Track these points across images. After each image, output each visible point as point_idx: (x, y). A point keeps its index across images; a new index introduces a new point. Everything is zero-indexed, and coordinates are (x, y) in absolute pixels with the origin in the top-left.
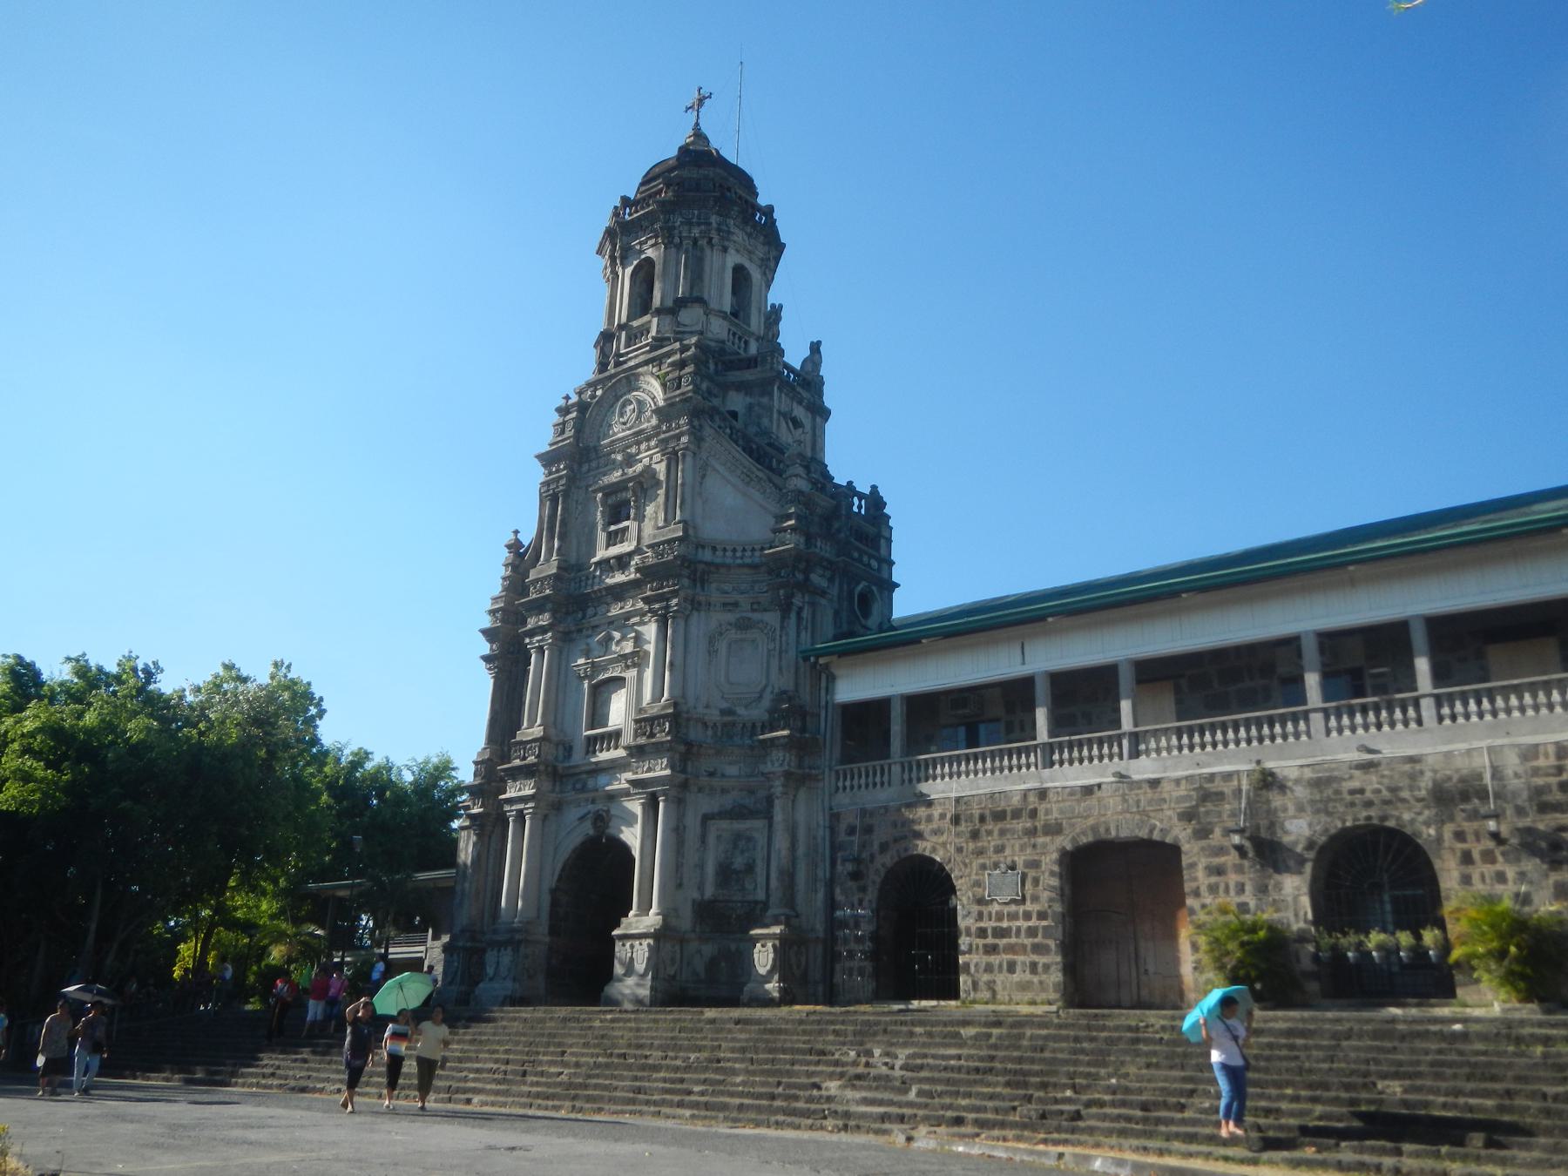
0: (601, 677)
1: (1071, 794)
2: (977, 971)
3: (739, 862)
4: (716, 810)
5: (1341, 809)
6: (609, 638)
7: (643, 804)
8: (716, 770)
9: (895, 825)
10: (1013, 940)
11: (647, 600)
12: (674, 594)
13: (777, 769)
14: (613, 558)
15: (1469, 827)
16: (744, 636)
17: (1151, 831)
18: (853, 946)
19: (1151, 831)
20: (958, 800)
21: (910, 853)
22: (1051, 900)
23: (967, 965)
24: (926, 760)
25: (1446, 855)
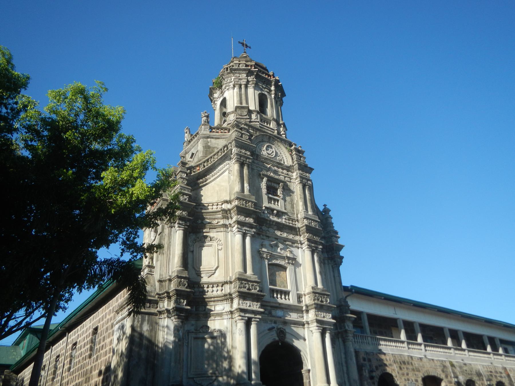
0: (274, 262)
1: (418, 359)
5: (465, 374)
6: (277, 246)
7: (320, 332)
9: (377, 360)
11: (309, 240)
12: (321, 244)
14: (276, 210)
20: (392, 354)
21: (385, 372)
24: (378, 338)
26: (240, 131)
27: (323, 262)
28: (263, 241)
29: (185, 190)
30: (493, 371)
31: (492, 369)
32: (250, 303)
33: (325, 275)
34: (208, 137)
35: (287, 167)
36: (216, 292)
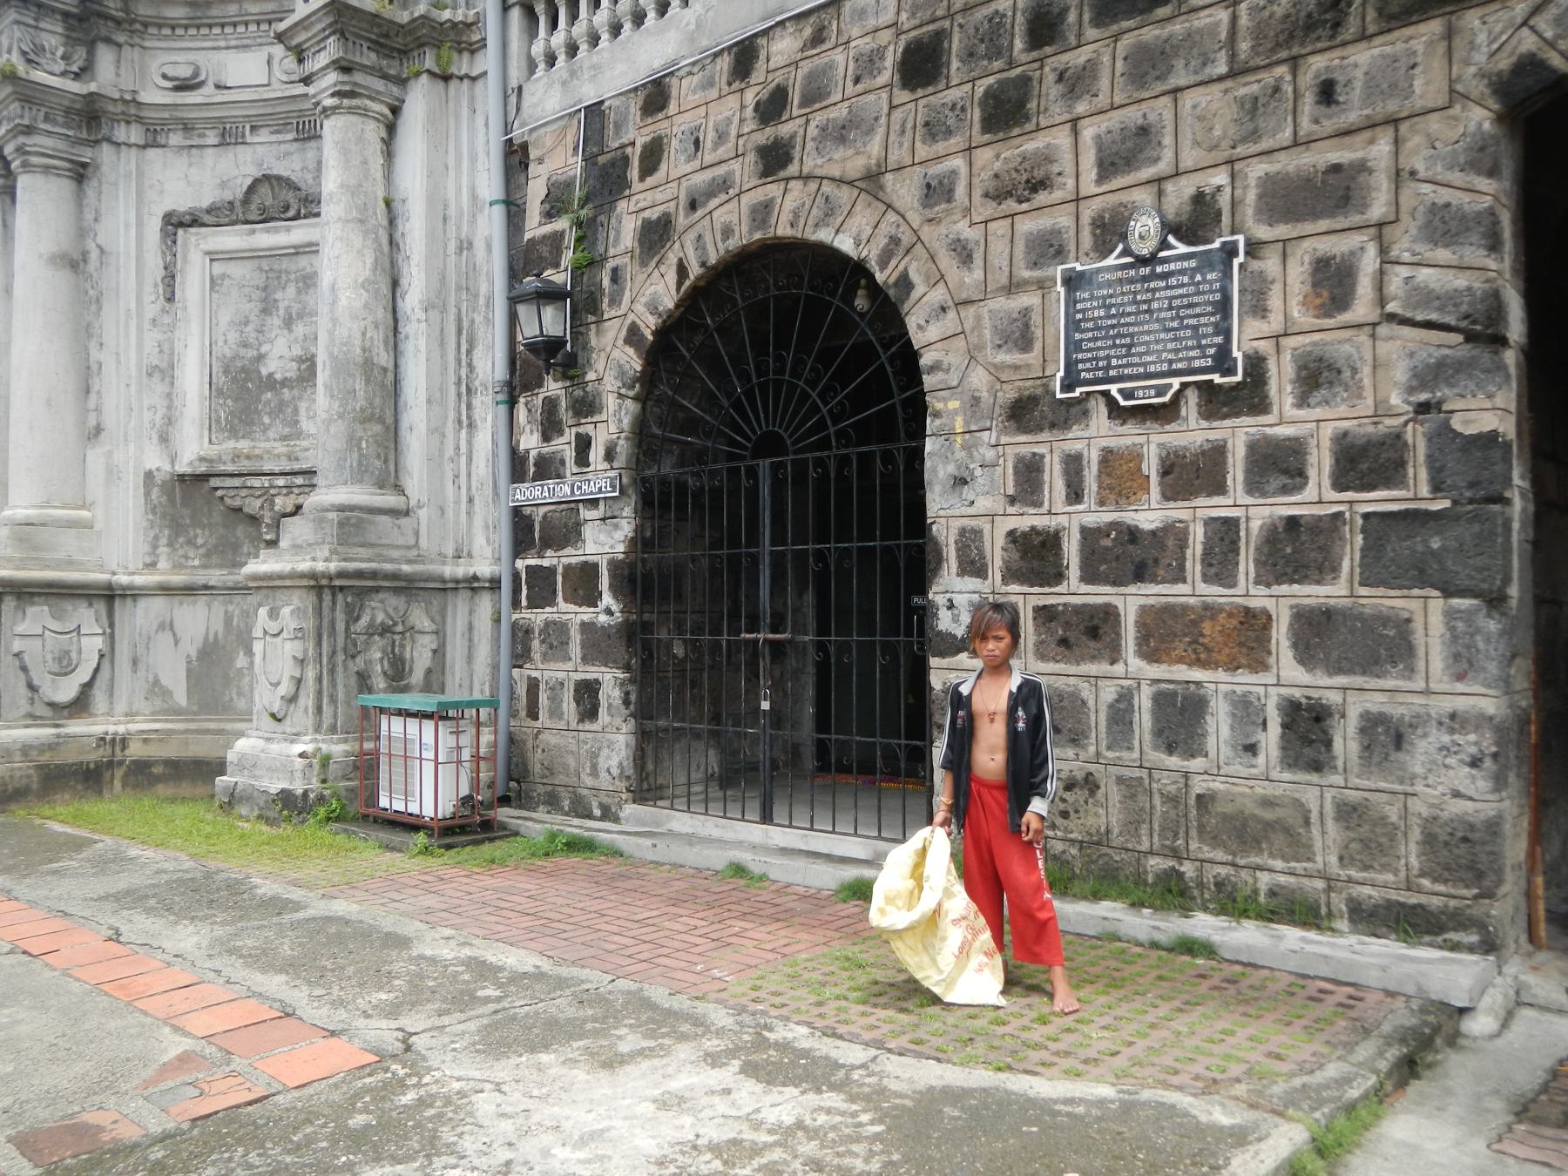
8: (196, 74)
10: (1194, 590)
22: (1431, 375)
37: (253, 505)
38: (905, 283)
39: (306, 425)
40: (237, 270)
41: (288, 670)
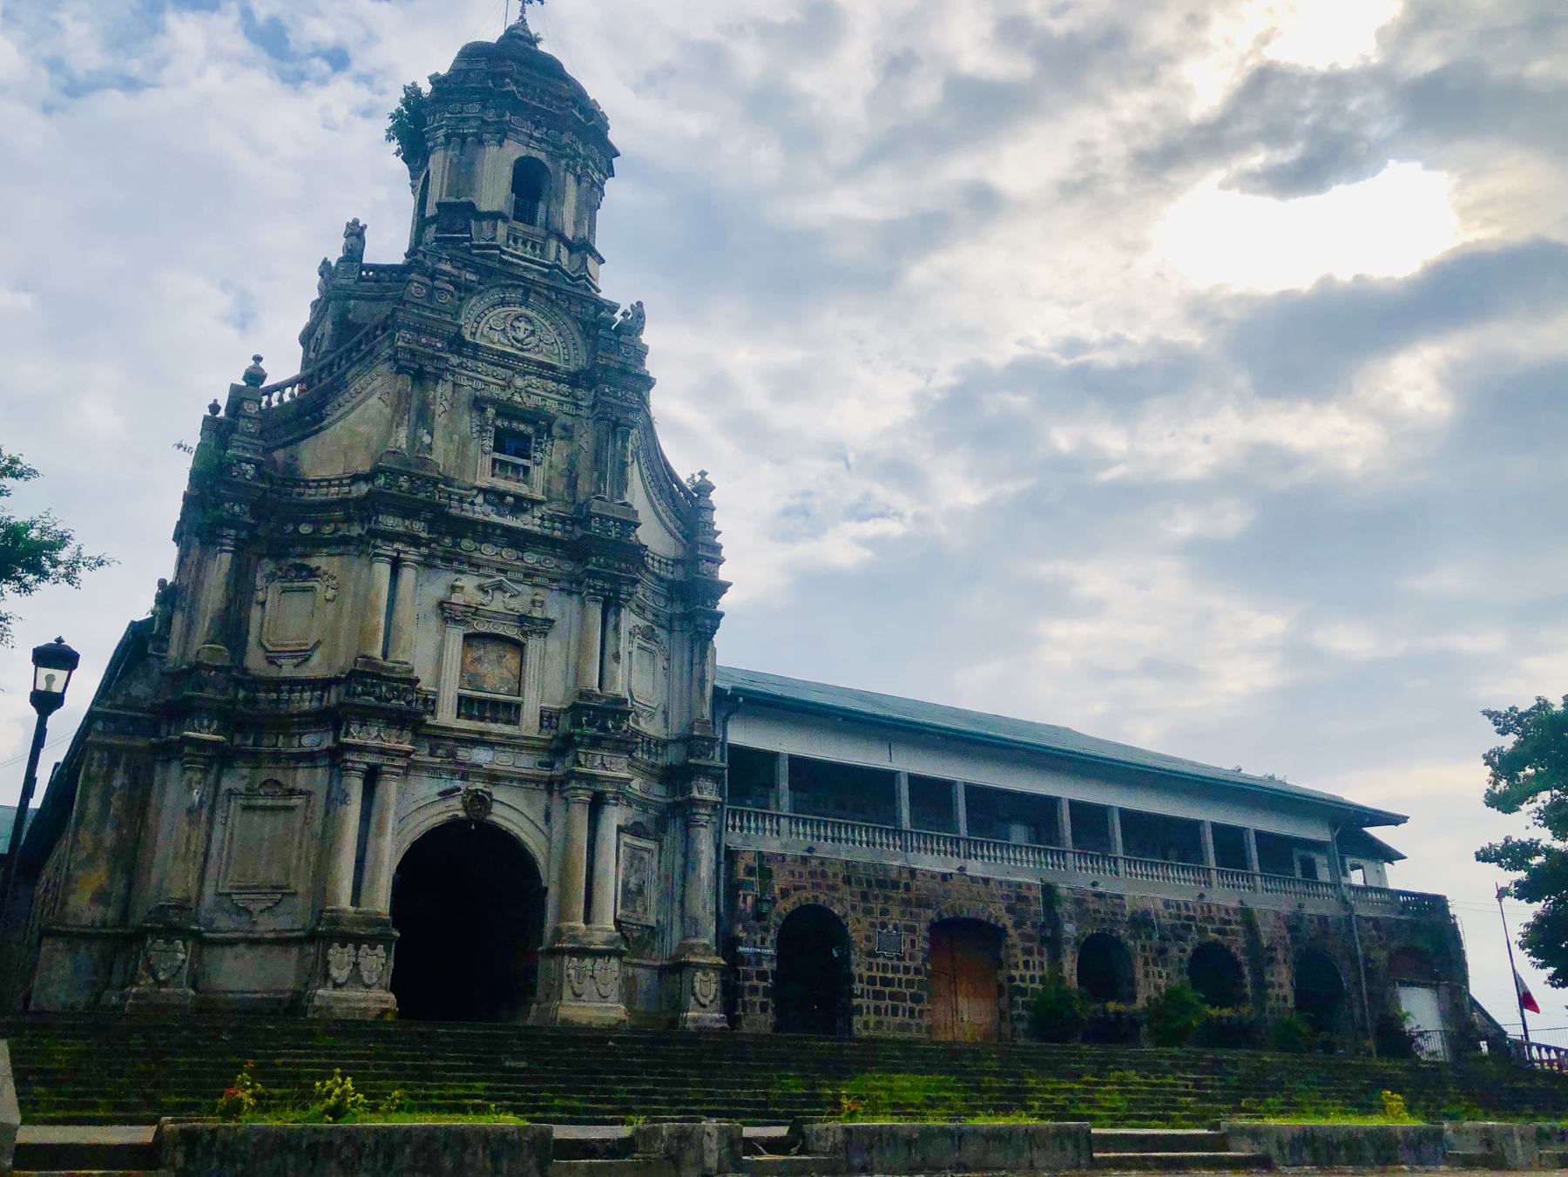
2: (868, 1012)
3: (633, 880)
4: (622, 823)
10: (896, 989)
13: (706, 796)
15: (1148, 943)
16: (646, 645)
17: (990, 917)
18: (755, 982)
19: (990, 917)
20: (847, 862)
22: (924, 960)
23: (859, 1007)
25: (1139, 958)
26: (428, 281)
27: (667, 625)
28: (458, 576)
29: (248, 450)
30: (1198, 915)
31: (1195, 910)
32: (379, 731)
33: (668, 660)
34: (350, 297)
35: (568, 373)
36: (307, 704)
37: (628, 935)
38: (847, 923)
39: (638, 909)
40: (627, 850)
41: (713, 992)
